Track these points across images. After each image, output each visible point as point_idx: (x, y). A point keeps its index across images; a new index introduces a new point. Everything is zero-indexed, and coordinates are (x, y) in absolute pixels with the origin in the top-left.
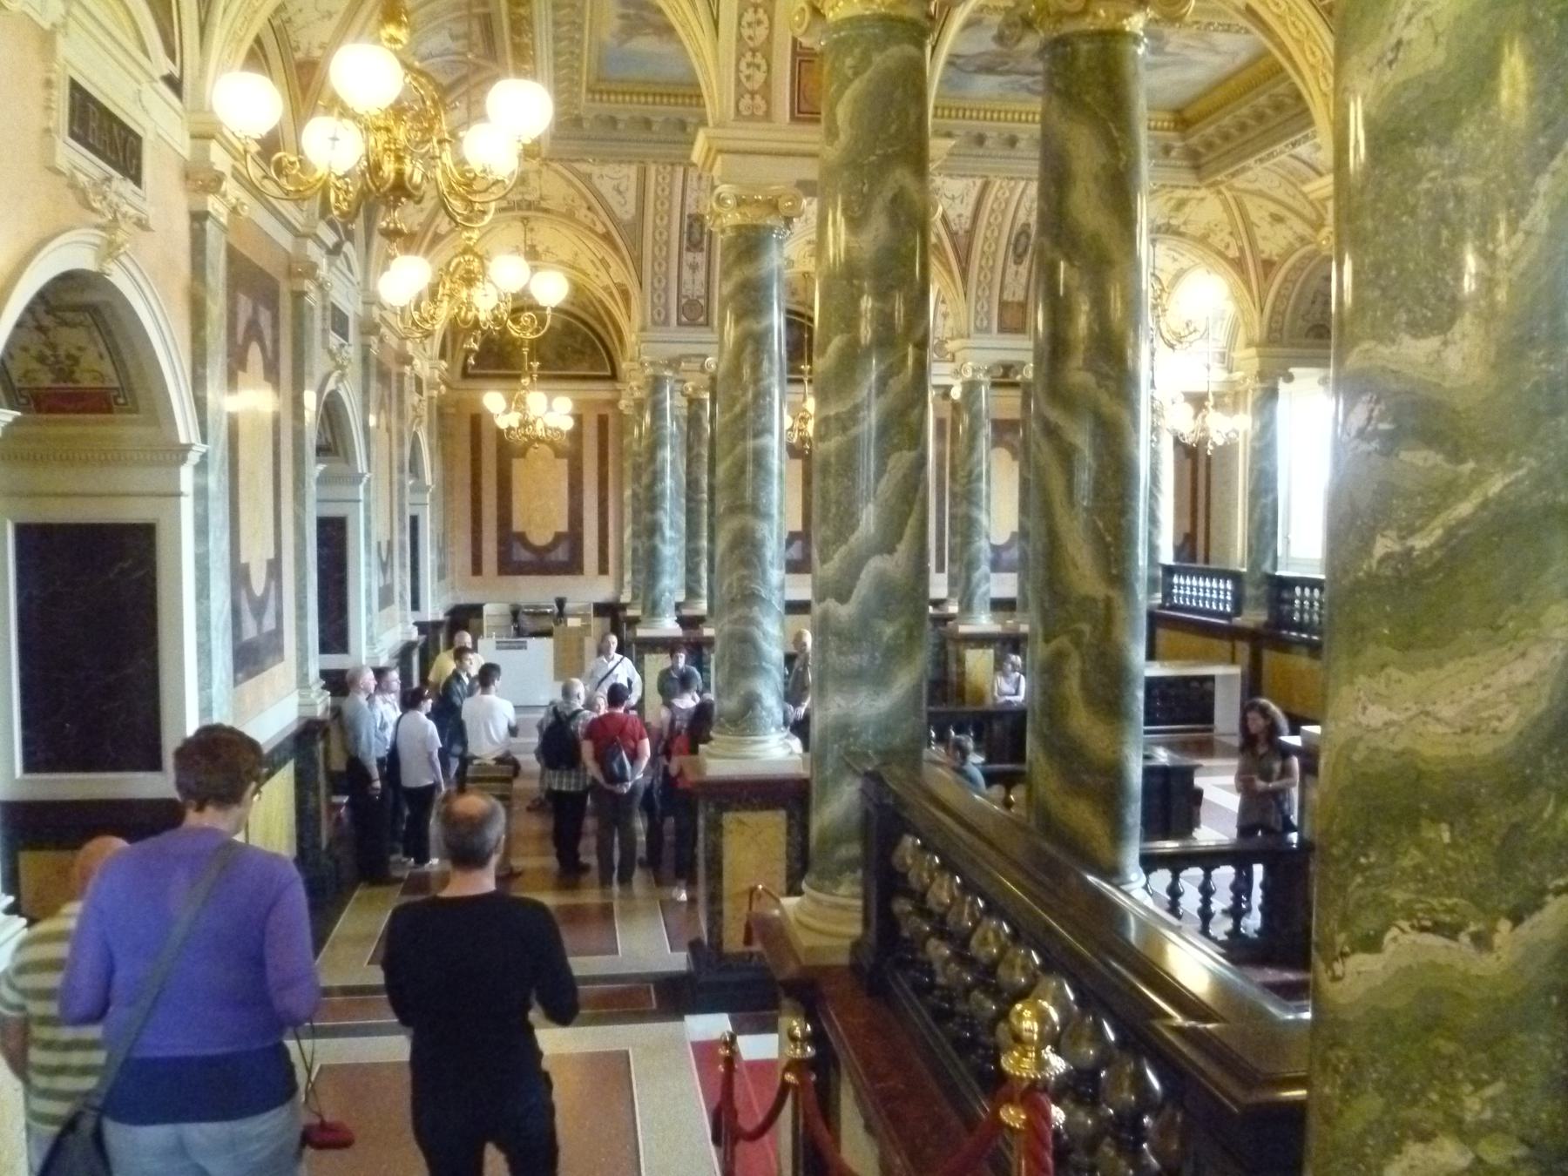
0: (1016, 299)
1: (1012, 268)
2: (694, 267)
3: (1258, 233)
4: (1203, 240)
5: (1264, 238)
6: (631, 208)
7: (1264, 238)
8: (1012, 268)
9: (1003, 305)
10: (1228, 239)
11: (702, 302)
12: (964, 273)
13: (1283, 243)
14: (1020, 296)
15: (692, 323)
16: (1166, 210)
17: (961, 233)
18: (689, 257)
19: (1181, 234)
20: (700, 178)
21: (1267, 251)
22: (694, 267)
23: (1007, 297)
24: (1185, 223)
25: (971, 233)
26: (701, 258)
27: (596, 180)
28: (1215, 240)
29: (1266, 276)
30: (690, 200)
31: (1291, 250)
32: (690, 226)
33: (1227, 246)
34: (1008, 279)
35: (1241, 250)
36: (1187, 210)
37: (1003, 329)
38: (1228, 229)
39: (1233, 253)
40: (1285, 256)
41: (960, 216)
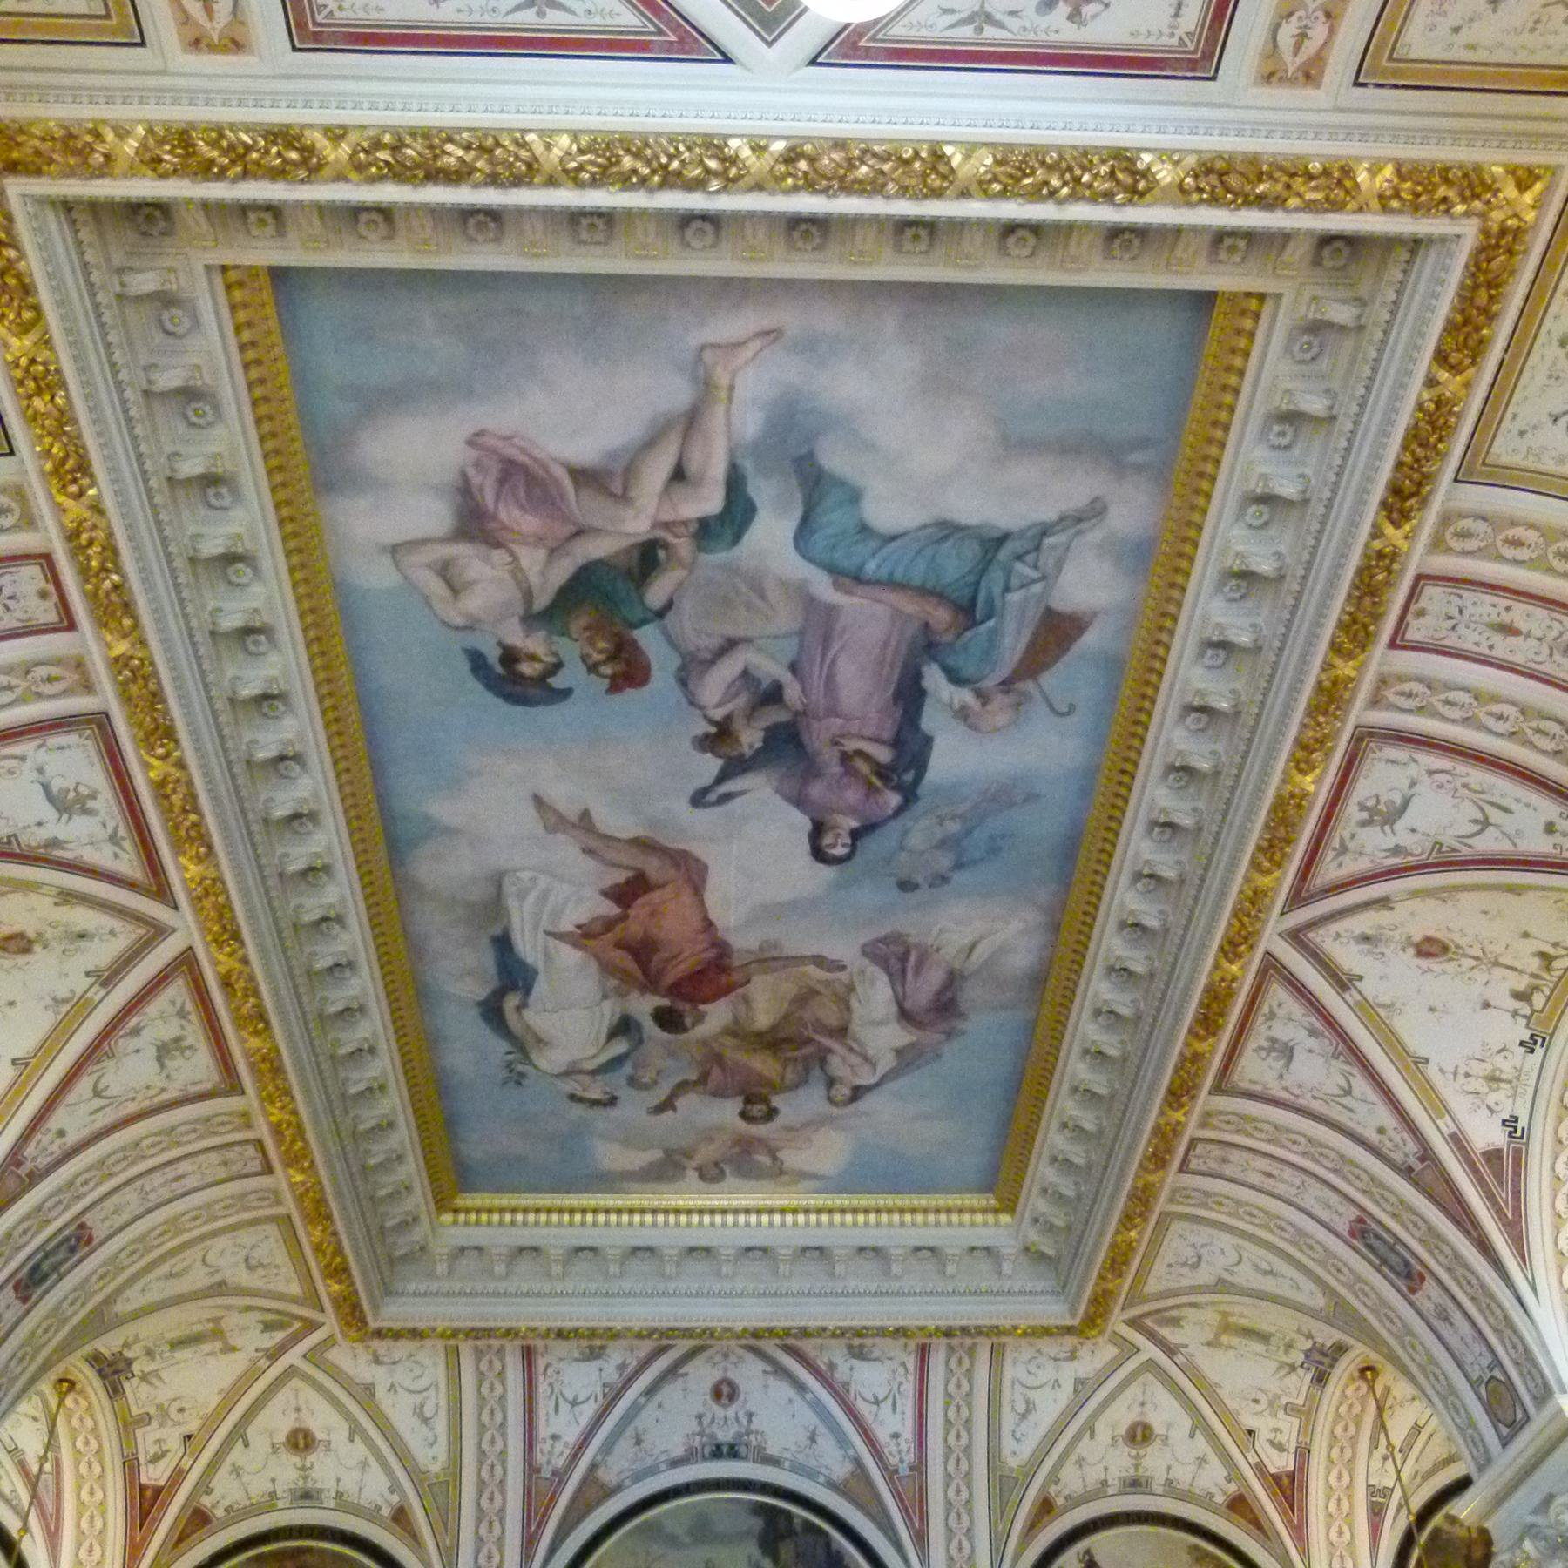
3: (237, 1454)
4: (128, 1425)
5: (236, 1471)
7: (236, 1471)
10: (174, 1443)
13: (258, 1487)
16: (170, 1335)
17: (23, 1171)
19: (115, 1391)
21: (216, 1495)
24: (145, 1378)
28: (146, 1440)
29: (180, 1540)
31: (269, 1503)
33: (155, 1459)
35: (178, 1476)
36: (183, 1354)
38: (193, 1426)
39: (154, 1475)
40: (234, 1515)
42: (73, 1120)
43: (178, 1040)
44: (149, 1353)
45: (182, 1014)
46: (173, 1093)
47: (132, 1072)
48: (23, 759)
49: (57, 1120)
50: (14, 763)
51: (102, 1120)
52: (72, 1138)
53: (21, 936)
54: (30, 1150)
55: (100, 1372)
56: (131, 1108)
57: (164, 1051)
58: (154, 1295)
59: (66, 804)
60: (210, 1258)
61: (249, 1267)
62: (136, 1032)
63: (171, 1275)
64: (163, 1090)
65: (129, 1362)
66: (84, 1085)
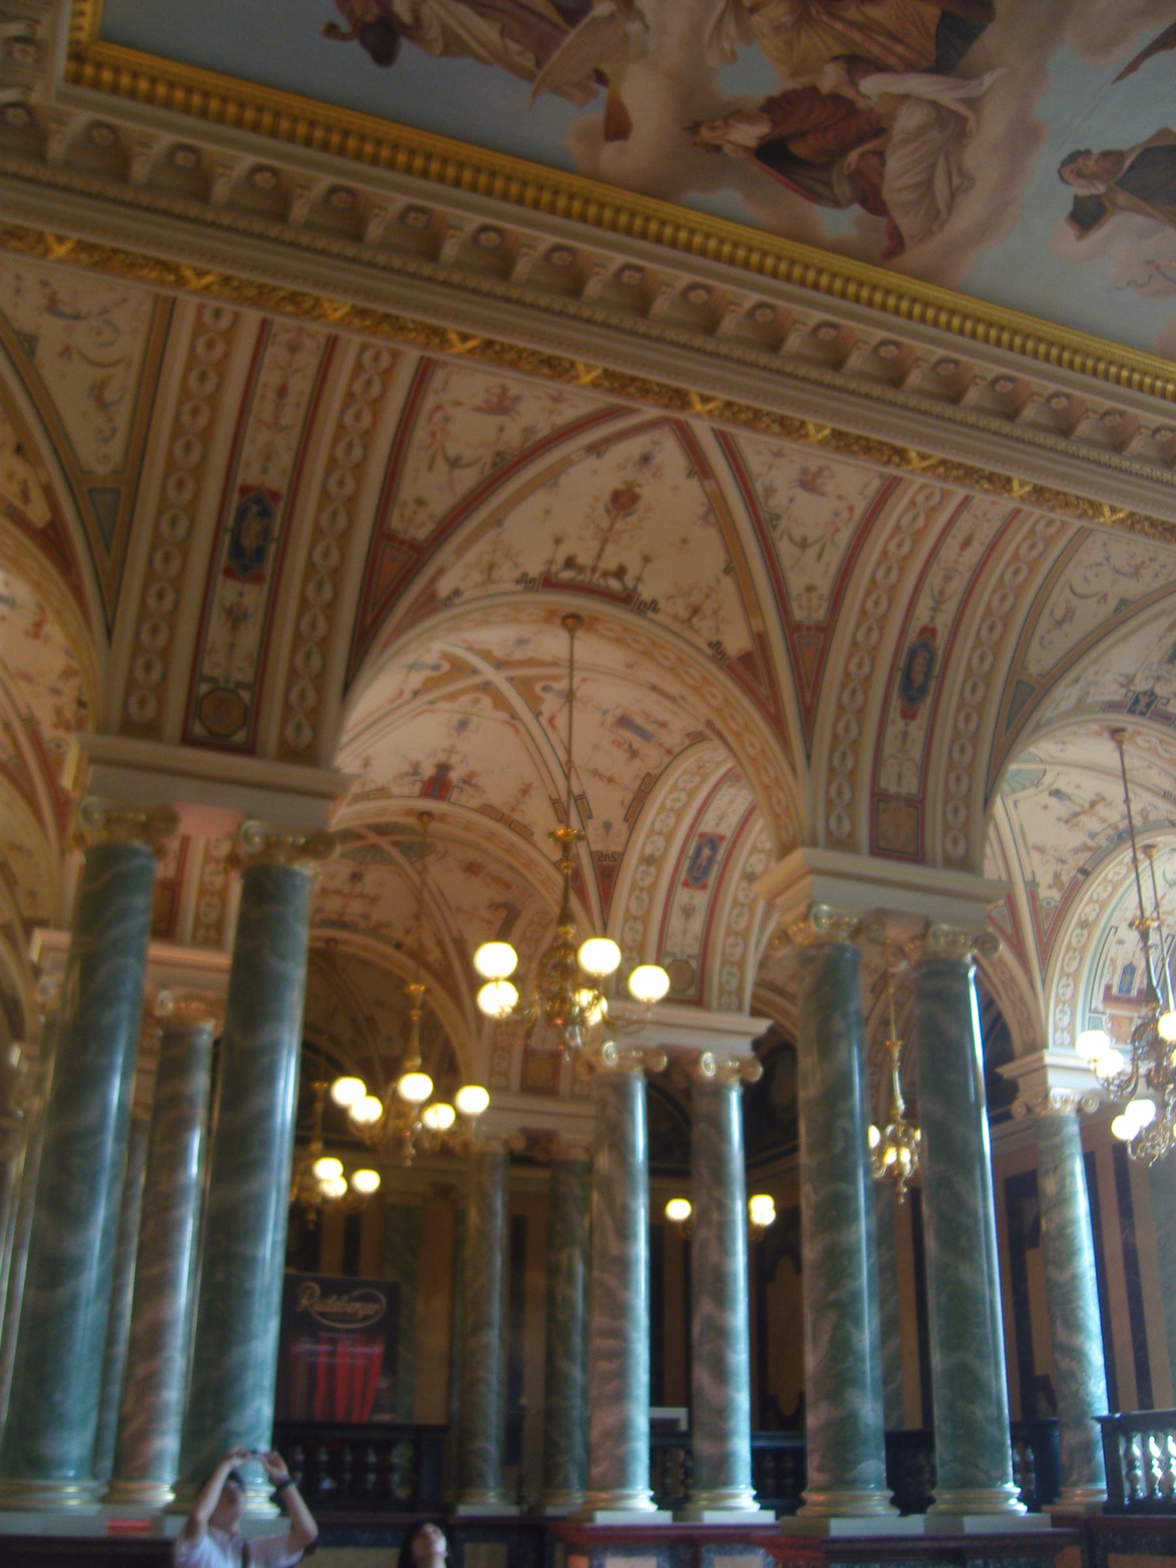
0: (904, 790)
1: (896, 725)
2: (236, 617)
6: (116, 450)
8: (896, 725)
9: (879, 797)
11: (246, 696)
12: (808, 715)
14: (910, 786)
15: (217, 743)
18: (227, 591)
20: (282, 391)
22: (236, 617)
23: (888, 782)
25: (826, 630)
26: (253, 597)
27: (46, 353)
30: (249, 451)
32: (242, 514)
34: (889, 749)
37: (878, 851)
41: (810, 589)
42: (810, 575)
43: (804, 471)
44: (1158, 679)
45: (778, 454)
46: (860, 507)
47: (806, 514)
48: (438, 408)
49: (795, 583)
50: (438, 416)
51: (834, 557)
52: (825, 586)
53: (616, 496)
54: (798, 614)
55: (1131, 711)
56: (845, 536)
57: (809, 483)
58: (1063, 641)
59: (501, 405)
60: (1081, 588)
61: (1136, 572)
62: (770, 491)
63: (1059, 623)
64: (851, 509)
65: (1151, 694)
66: (786, 551)
